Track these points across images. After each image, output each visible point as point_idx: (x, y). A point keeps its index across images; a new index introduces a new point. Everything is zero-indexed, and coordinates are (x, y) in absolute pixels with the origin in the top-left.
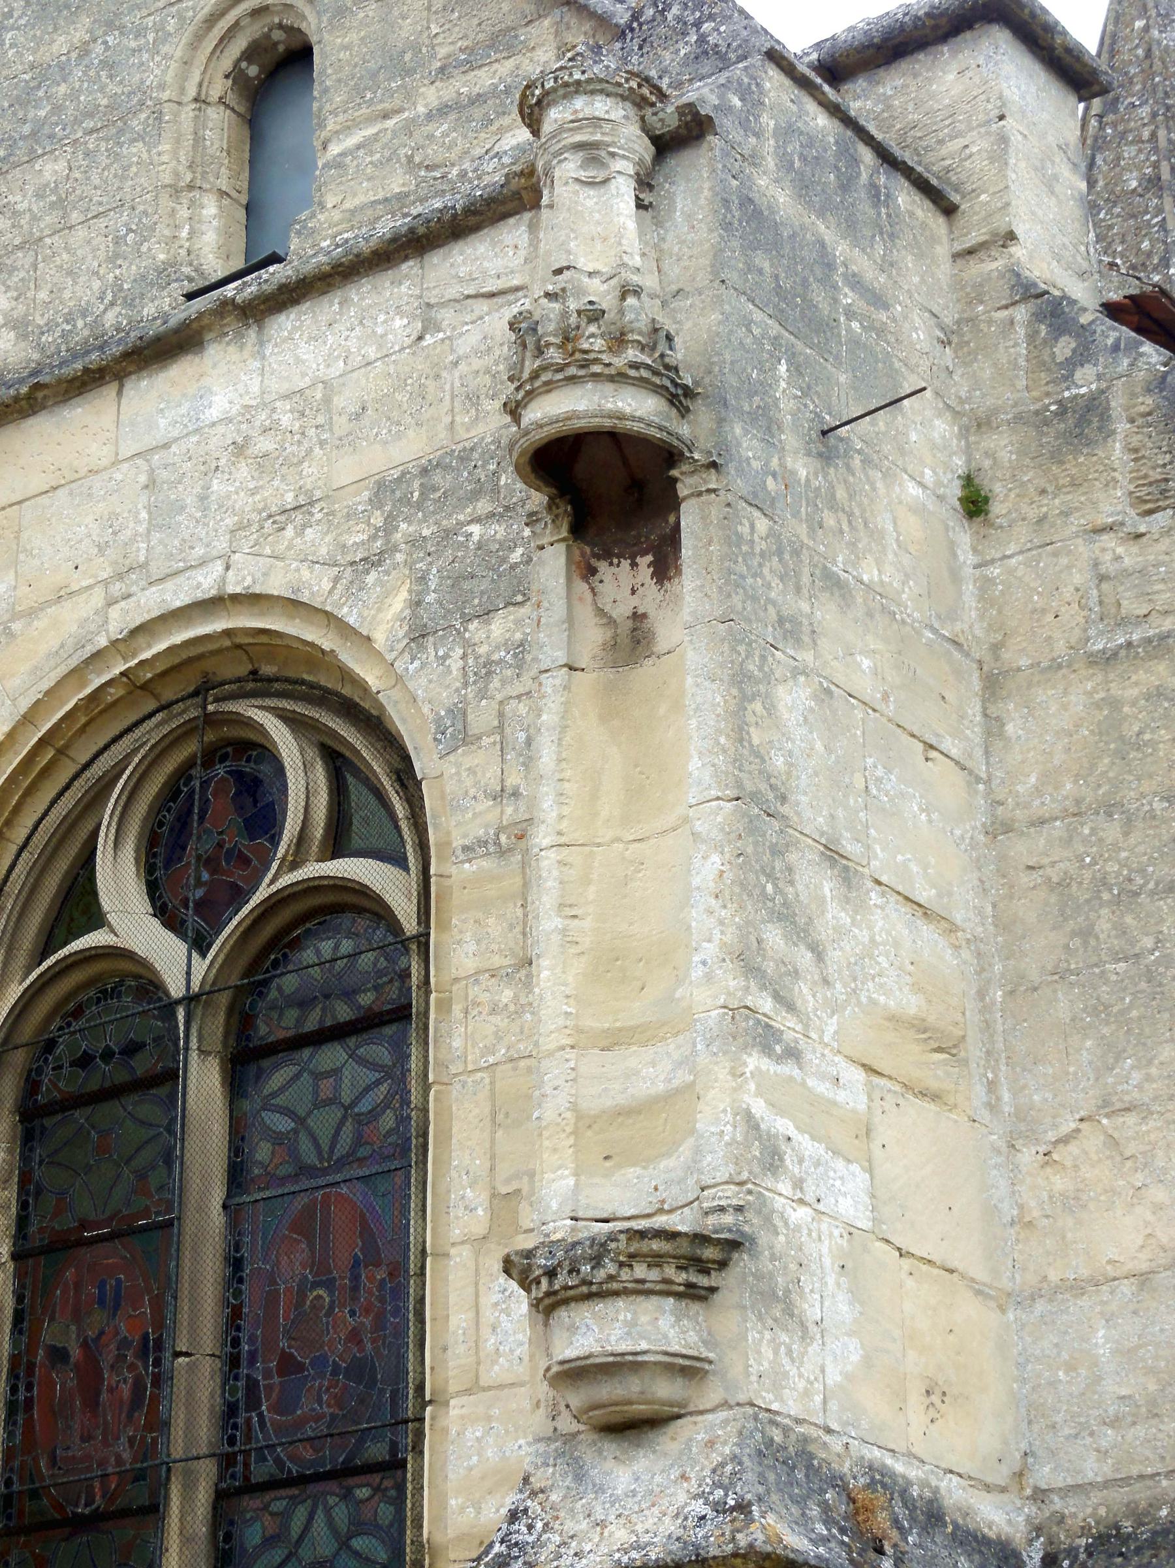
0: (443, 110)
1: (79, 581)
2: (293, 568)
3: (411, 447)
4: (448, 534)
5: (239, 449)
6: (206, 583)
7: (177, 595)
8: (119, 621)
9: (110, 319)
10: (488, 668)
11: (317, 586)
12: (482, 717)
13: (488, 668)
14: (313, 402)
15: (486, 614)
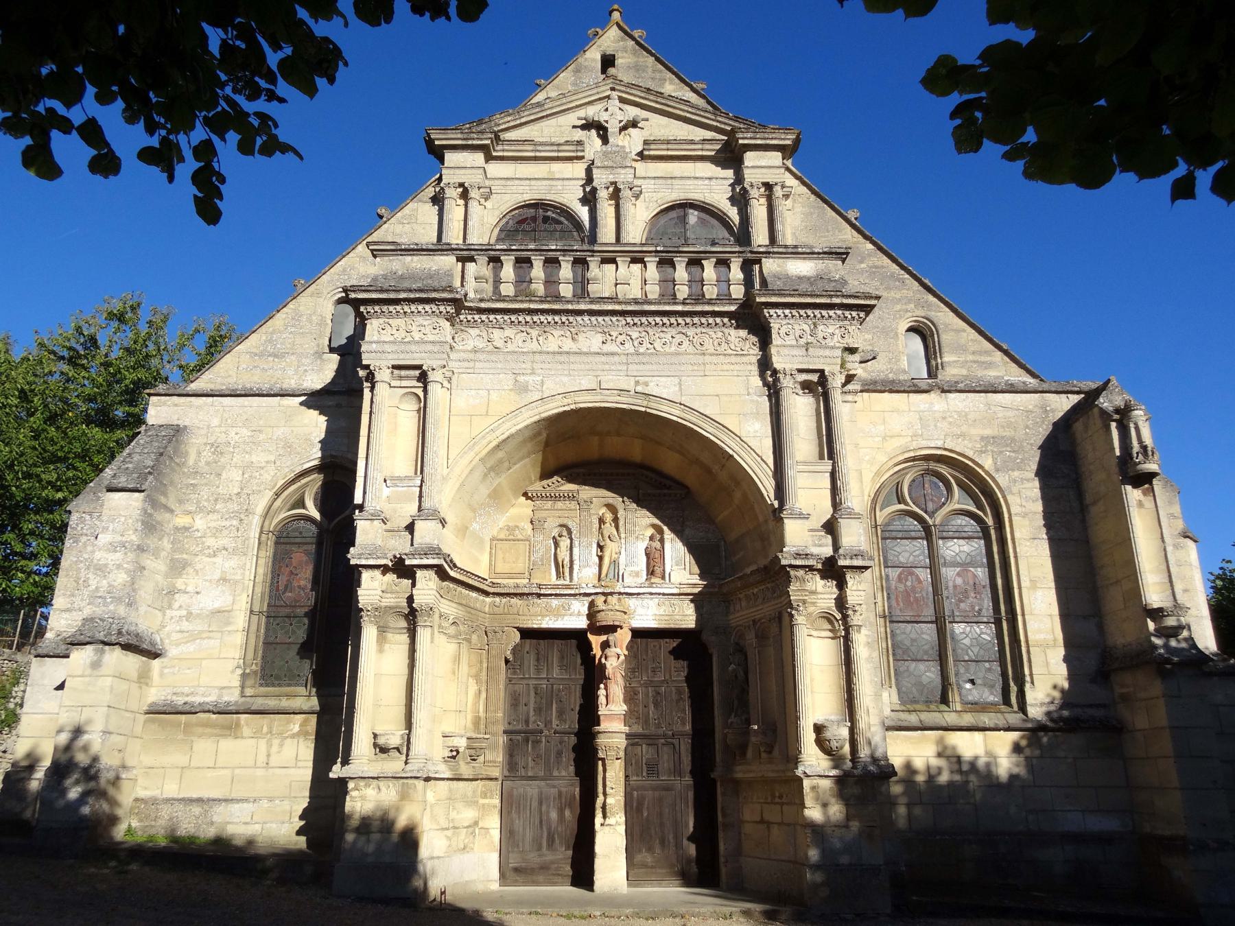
0: (975, 362)
1: (903, 433)
2: (965, 447)
3: (988, 432)
4: (1001, 452)
5: (944, 418)
6: (940, 444)
7: (924, 443)
8: (914, 445)
9: (891, 376)
10: (1015, 481)
11: (970, 454)
12: (1015, 490)
13: (1015, 481)
14: (964, 415)
15: (1013, 470)
